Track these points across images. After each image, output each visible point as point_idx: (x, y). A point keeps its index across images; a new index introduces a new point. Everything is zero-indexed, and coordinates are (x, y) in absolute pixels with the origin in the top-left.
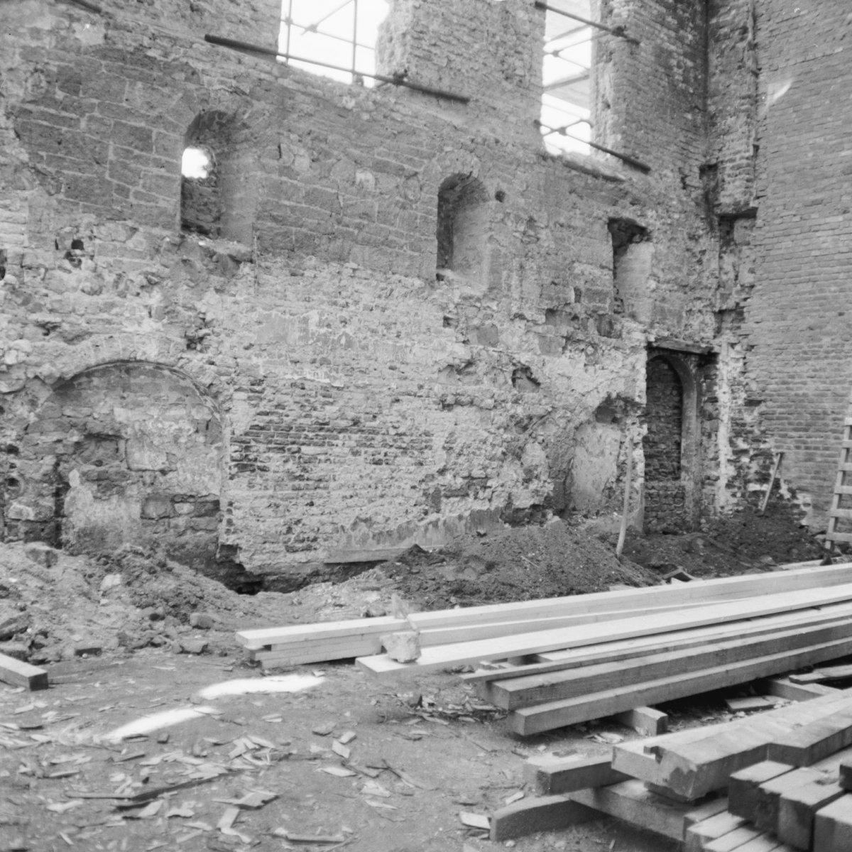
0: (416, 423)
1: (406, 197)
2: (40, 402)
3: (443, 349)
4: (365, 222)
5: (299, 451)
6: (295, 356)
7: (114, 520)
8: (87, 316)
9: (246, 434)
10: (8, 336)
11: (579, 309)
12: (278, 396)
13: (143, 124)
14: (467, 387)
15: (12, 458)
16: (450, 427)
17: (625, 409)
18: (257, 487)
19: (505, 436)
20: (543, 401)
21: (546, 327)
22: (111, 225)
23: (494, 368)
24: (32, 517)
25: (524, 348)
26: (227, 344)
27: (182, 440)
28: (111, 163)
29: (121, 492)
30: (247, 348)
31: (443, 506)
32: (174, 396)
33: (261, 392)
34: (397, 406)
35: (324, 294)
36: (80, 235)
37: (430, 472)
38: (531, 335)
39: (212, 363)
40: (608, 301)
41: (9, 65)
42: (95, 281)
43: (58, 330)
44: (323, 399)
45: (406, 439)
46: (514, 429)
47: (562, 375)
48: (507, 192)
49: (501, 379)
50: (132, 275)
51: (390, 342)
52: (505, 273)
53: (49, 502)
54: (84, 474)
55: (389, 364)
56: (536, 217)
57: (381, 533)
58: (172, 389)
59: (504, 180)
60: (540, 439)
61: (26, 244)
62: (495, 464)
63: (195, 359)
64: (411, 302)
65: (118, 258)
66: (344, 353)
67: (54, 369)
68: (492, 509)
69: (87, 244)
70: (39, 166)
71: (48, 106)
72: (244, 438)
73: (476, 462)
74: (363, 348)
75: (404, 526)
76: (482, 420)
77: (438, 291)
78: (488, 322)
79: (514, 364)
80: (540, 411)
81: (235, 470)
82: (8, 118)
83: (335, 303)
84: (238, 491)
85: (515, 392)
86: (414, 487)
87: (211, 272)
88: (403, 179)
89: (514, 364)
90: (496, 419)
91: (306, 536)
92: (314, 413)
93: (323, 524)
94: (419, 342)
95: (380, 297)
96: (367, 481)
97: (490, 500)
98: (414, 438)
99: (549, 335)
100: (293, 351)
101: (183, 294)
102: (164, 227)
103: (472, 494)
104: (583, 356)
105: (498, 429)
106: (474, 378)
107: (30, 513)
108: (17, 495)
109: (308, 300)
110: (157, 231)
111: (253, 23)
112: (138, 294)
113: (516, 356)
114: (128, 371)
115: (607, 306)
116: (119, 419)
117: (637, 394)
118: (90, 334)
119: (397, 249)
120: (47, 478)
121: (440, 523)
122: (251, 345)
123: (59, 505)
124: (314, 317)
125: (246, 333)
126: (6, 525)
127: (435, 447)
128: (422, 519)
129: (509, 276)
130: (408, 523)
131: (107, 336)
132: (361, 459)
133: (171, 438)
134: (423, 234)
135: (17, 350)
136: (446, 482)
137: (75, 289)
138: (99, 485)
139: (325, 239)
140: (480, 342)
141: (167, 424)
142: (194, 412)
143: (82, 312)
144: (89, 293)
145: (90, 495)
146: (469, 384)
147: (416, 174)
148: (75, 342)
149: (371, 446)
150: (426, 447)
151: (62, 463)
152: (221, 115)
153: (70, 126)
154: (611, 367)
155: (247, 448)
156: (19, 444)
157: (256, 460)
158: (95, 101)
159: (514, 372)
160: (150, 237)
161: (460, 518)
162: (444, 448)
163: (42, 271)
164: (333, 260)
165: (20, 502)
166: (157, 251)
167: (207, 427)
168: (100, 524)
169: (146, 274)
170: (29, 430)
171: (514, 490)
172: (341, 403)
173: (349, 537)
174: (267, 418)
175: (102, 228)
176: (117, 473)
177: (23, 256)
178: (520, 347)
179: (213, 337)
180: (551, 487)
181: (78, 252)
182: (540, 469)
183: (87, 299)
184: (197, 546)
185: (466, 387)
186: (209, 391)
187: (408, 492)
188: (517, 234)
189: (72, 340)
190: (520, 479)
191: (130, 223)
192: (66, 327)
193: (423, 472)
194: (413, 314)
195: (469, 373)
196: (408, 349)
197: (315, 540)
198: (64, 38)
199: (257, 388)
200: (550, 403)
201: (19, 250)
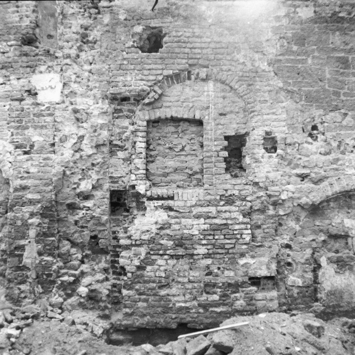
2: (302, 219)
7: (348, 285)
10: (282, 184)
13: (343, 55)
15: (288, 251)
22: (332, 114)
24: (301, 285)
28: (328, 79)
36: (315, 122)
41: (266, 38)
42: (327, 147)
43: (309, 177)
50: (348, 141)
53: (310, 275)
54: (329, 259)
61: (287, 132)
65: (338, 132)
67: (308, 200)
70: (289, 88)
71: (290, 55)
82: (269, 66)
107: (300, 282)
108: (292, 271)
112: (352, 151)
114: (350, 197)
116: (347, 226)
118: (328, 177)
120: (308, 262)
123: (316, 277)
126: (286, 289)
131: (337, 178)
135: (287, 191)
137: (316, 153)
138: (338, 265)
143: (321, 166)
144: (324, 155)
145: (333, 271)
148: (319, 183)
151: (316, 253)
153: (303, 63)
156: (291, 243)
158: (315, 47)
163: (297, 145)
165: (294, 276)
168: (339, 287)
170: (297, 235)
175: (327, 116)
176: (348, 257)
177: (286, 138)
181: (315, 132)
183: (323, 158)
189: (317, 182)
191: (343, 111)
192: (313, 175)
198: (292, 18)
201: (284, 136)
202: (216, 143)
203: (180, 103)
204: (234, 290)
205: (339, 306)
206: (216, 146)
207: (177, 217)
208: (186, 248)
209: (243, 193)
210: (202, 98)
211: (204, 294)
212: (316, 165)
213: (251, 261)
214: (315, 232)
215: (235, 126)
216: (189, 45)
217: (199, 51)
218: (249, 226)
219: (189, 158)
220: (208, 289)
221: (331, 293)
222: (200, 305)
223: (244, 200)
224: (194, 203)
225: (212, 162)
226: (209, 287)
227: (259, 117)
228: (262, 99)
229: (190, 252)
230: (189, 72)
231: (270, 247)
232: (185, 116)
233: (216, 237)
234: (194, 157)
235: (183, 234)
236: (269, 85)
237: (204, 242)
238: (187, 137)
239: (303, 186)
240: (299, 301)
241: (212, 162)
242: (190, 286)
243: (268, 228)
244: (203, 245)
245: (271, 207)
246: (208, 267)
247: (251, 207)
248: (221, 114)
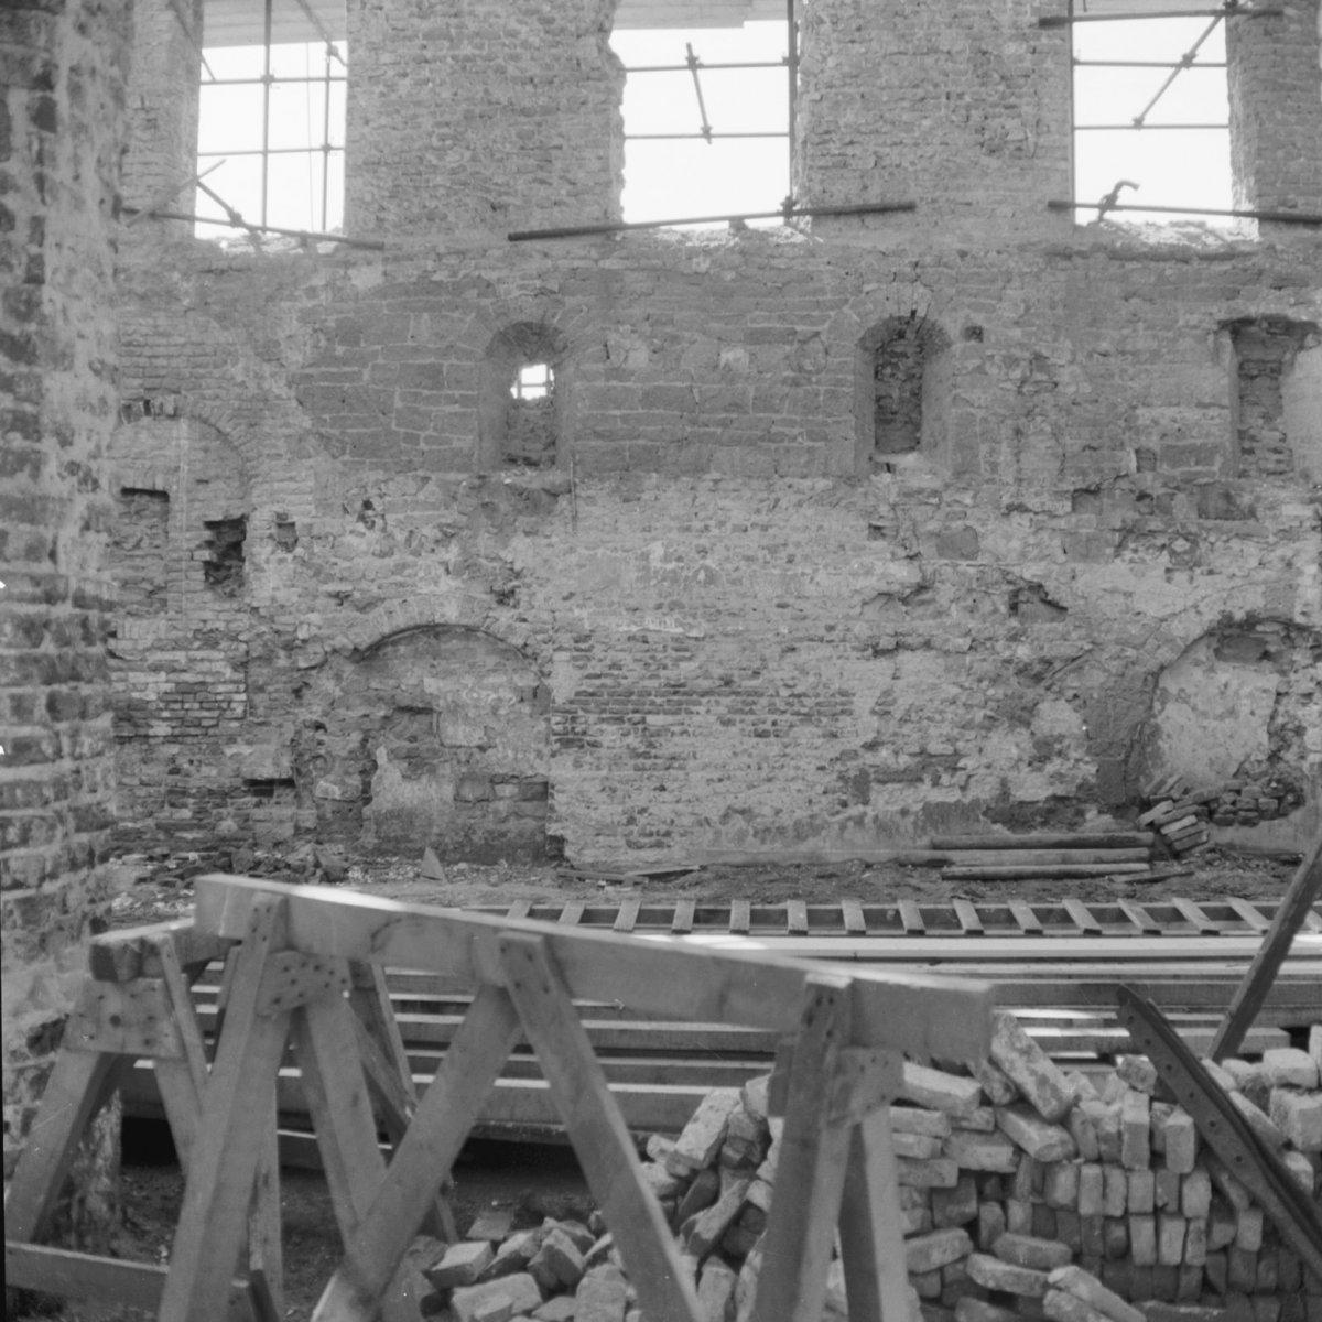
0: (824, 679)
1: (800, 369)
3: (868, 572)
4: (734, 416)
5: (643, 721)
6: (632, 603)
8: (378, 582)
9: (571, 702)
11: (1149, 482)
12: (611, 653)
13: (432, 360)
14: (920, 623)
15: (320, 735)
16: (884, 681)
17: (1288, 636)
18: (586, 767)
19: (991, 692)
20: (1074, 635)
21: (1074, 519)
22: (400, 478)
23: (970, 591)
24: (338, 797)
25: (1031, 556)
26: (540, 596)
27: (502, 712)
28: (398, 411)
29: (433, 771)
30: (565, 599)
31: (873, 796)
32: (491, 661)
33: (589, 650)
34: (791, 657)
35: (672, 519)
37: (849, 747)
38: (1045, 535)
39: (525, 620)
40: (1218, 460)
44: (674, 654)
45: (806, 701)
46: (1014, 680)
47: (1113, 591)
48: (985, 326)
49: (986, 606)
51: (776, 572)
52: (984, 448)
53: (355, 781)
55: (776, 601)
56: (1045, 352)
57: (767, 830)
58: (488, 653)
59: (978, 308)
60: (1070, 693)
62: (971, 734)
63: (504, 616)
64: (810, 512)
66: (703, 592)
67: (345, 641)
68: (966, 801)
69: (376, 502)
70: (323, 430)
71: (329, 365)
72: (568, 707)
73: (933, 731)
74: (733, 582)
75: (805, 821)
76: (948, 669)
77: (861, 490)
78: (957, 525)
79: (1010, 582)
80: (1067, 650)
81: (556, 746)
83: (688, 529)
84: (561, 770)
85: (1014, 622)
86: (821, 768)
87: (520, 512)
88: (796, 346)
89: (1010, 582)
90: (976, 665)
91: (654, 829)
92: (662, 673)
93: (678, 814)
94: (826, 567)
95: (758, 511)
96: (745, 759)
97: (963, 788)
98: (821, 699)
99: (1083, 531)
100: (630, 596)
101: (484, 542)
102: (459, 470)
103: (927, 778)
104: (1165, 557)
105: (980, 680)
106: (931, 608)
107: (336, 792)
108: (326, 772)
109: (648, 530)
110: (452, 476)
111: (572, 200)
113: (1016, 570)
114: (437, 636)
115: (1216, 468)
116: (428, 691)
117: (1298, 608)
118: (383, 600)
119: (786, 444)
121: (866, 820)
122: (572, 595)
123: (367, 787)
124: (657, 550)
125: (565, 580)
127: (856, 714)
128: (838, 813)
129: (992, 451)
130: (812, 817)
132: (733, 730)
133: (488, 709)
134: (830, 415)
136: (877, 761)
137: (366, 553)
139: (672, 449)
140: (941, 555)
141: (484, 693)
142: (516, 678)
146: (921, 618)
147: (817, 334)
149: (752, 712)
150: (843, 712)
152: (528, 325)
154: (1234, 569)
155: (574, 719)
156: (324, 720)
157: (584, 733)
158: (379, 347)
159: (1015, 594)
160: (444, 485)
161: (904, 812)
162: (873, 712)
164: (685, 473)
166: (454, 498)
167: (535, 695)
169: (440, 527)
171: (1012, 775)
172: (702, 657)
173: (717, 833)
174: (598, 682)
177: (311, 525)
178: (1023, 555)
179: (524, 590)
180: (1093, 769)
181: (370, 513)
182: (1066, 742)
183: (378, 562)
184: (521, 835)
185: (917, 623)
186: (524, 654)
187: (812, 775)
188: (1009, 385)
190: (1026, 758)
191: (421, 473)
192: (357, 595)
193: (835, 748)
194: (814, 528)
195: (923, 603)
196: (807, 579)
197: (668, 834)
198: (340, 289)
199: (583, 646)
200: (1089, 636)
201: (307, 520)
202: (188, 535)
203: (129, 461)
204: (218, 801)
205: (407, 839)
206: (189, 540)
207: (121, 669)
208: (136, 726)
209: (233, 626)
210: (167, 453)
211: (167, 807)
212: (364, 576)
213: (246, 750)
214: (368, 701)
215: (223, 503)
216: (147, 351)
217: (165, 363)
218: (242, 687)
219: (149, 560)
220: (173, 798)
221: (396, 814)
222: (159, 827)
223: (235, 639)
224: (149, 644)
225: (180, 570)
226: (176, 796)
227: (266, 486)
228: (274, 451)
229: (142, 731)
230: (147, 403)
231: (280, 726)
232: (139, 486)
233: (187, 706)
234: (156, 560)
235: (131, 699)
236: (287, 425)
237: (166, 714)
238: (144, 523)
239: (338, 615)
240: (335, 827)
241: (180, 570)
242: (142, 792)
243: (277, 691)
244: (164, 719)
245: (282, 654)
246: (173, 759)
247: (247, 653)
248: (200, 481)
